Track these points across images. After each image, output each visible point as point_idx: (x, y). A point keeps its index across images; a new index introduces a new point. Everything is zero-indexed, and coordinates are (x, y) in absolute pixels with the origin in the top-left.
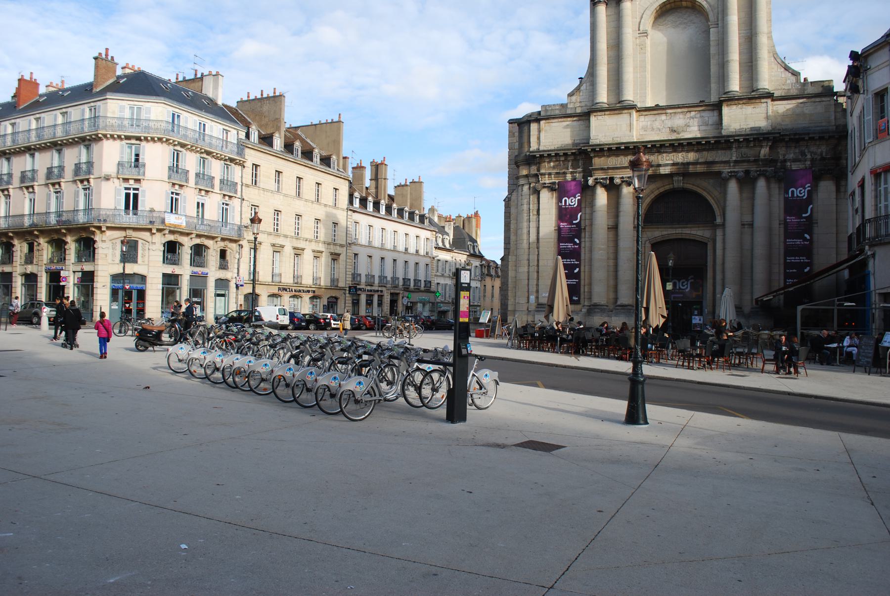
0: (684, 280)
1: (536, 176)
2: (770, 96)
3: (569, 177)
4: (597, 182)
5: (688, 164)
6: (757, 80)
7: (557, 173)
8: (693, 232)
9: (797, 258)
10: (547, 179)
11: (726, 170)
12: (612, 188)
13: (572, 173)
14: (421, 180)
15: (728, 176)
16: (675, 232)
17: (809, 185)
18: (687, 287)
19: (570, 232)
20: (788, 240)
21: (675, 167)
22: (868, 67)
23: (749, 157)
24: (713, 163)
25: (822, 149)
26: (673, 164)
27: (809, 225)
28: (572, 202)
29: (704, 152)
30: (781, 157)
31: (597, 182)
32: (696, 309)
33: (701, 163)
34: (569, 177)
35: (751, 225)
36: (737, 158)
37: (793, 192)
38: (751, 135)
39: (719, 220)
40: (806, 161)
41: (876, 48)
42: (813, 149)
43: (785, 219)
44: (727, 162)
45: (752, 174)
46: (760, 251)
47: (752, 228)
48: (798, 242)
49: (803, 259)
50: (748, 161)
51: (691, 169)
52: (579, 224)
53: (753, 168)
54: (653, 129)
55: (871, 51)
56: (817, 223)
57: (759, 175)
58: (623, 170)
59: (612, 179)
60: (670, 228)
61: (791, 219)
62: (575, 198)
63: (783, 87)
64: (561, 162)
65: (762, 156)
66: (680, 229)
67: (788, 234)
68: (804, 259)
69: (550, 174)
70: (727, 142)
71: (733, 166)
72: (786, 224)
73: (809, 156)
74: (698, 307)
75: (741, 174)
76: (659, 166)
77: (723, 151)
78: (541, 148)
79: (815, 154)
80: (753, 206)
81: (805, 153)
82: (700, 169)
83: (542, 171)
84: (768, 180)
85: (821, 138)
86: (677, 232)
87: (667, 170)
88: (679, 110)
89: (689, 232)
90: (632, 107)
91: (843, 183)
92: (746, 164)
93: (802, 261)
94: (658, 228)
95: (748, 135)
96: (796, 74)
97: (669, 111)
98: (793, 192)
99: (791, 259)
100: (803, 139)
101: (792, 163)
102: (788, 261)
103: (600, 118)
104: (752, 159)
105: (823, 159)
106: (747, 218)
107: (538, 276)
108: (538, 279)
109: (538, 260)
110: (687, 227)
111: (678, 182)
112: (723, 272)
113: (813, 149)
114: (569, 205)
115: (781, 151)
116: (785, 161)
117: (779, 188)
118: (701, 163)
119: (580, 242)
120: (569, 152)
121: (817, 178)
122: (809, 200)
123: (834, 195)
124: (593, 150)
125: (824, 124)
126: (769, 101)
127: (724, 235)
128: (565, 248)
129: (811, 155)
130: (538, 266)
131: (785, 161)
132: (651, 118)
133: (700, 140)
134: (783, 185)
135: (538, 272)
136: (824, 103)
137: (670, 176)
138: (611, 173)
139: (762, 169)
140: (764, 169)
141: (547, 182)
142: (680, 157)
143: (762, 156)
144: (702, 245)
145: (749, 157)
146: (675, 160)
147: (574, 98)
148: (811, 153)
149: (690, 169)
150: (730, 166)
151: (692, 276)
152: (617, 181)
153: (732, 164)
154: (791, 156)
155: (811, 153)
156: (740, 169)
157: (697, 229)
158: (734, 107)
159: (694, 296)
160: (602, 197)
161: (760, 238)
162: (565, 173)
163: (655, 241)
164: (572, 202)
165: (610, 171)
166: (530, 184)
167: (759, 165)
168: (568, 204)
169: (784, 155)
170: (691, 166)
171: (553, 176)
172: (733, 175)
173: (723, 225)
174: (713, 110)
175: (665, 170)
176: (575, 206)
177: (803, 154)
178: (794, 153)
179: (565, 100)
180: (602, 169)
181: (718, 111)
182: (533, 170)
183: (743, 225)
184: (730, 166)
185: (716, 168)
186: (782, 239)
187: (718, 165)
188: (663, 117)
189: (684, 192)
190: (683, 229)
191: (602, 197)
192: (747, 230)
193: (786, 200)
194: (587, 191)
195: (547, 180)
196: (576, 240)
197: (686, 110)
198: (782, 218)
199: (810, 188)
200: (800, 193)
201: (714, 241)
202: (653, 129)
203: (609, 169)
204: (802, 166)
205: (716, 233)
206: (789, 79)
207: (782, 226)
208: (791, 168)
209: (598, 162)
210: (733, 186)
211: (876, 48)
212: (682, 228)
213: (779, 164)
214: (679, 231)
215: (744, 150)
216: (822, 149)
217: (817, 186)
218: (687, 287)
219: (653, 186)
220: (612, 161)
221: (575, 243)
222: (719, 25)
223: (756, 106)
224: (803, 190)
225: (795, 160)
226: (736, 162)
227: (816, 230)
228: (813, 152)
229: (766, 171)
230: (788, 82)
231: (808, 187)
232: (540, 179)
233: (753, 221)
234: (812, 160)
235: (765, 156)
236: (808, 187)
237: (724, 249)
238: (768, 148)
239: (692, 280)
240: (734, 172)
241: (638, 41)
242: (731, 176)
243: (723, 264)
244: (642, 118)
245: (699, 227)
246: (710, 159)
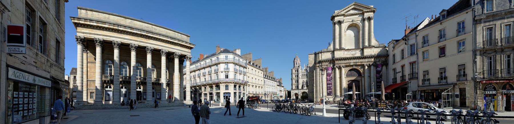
1: (321, 66)
2: (374, 47)
3: (329, 66)
4: (336, 67)
5: (357, 62)
6: (371, 43)
7: (326, 65)
12: (340, 68)
13: (330, 65)
24: (362, 62)
25: (383, 59)
26: (354, 62)
27: (381, 76)
31: (336, 67)
33: (360, 62)
34: (329, 66)
39: (363, 75)
42: (382, 59)
43: (376, 75)
48: (379, 80)
51: (358, 64)
54: (348, 54)
59: (340, 66)
67: (377, 79)
69: (324, 65)
72: (377, 76)
73: (381, 61)
76: (351, 63)
78: (322, 59)
82: (359, 64)
83: (322, 65)
85: (384, 57)
90: (344, 49)
97: (352, 50)
99: (378, 84)
111: (354, 67)
112: (364, 87)
113: (382, 59)
118: (360, 62)
120: (329, 60)
121: (382, 66)
122: (381, 71)
123: (386, 70)
124: (336, 59)
126: (374, 48)
127: (364, 79)
137: (352, 66)
138: (340, 65)
142: (355, 61)
152: (341, 67)
154: (377, 61)
158: (367, 49)
160: (337, 71)
162: (328, 65)
166: (319, 68)
173: (364, 77)
175: (352, 64)
177: (380, 60)
180: (338, 64)
182: (320, 64)
185: (363, 63)
186: (376, 79)
188: (350, 52)
191: (337, 71)
193: (376, 70)
194: (333, 69)
198: (376, 75)
200: (379, 69)
201: (362, 80)
202: (348, 54)
203: (339, 64)
204: (379, 63)
209: (336, 62)
217: (382, 68)
219: (348, 68)
220: (340, 62)
221: (331, 81)
225: (378, 62)
226: (367, 62)
227: (382, 77)
234: (382, 62)
241: (344, 33)
243: (364, 85)
244: (346, 52)
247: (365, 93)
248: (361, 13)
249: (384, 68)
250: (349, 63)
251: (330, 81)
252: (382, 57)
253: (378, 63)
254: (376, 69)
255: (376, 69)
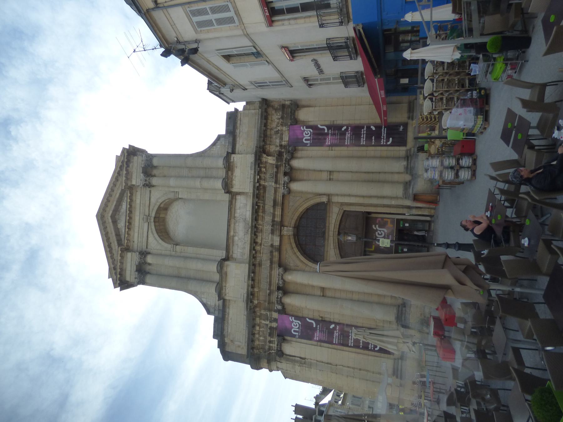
0: (377, 233)
5: (273, 221)
8: (334, 221)
9: (362, 137)
10: (274, 345)
11: (281, 191)
14: (294, 405)
15: (287, 189)
16: (332, 237)
17: (302, 127)
18: (383, 231)
19: (323, 331)
20: (346, 144)
21: (275, 232)
22: (176, 39)
23: (274, 172)
25: (275, 118)
28: (295, 326)
29: (266, 208)
30: (278, 149)
32: (404, 225)
35: (331, 172)
36: (273, 182)
37: (306, 140)
38: (255, 169)
39: (324, 199)
40: (282, 130)
41: (158, 32)
43: (329, 146)
44: (276, 190)
45: (288, 170)
46: (354, 165)
47: (333, 172)
49: (364, 131)
50: (277, 173)
51: (278, 219)
52: (317, 321)
53: (282, 169)
55: (160, 35)
56: (333, 121)
57: (289, 165)
58: (273, 276)
60: (328, 241)
61: (328, 142)
62: (293, 322)
63: (227, 147)
64: (261, 329)
65: (274, 162)
66: (330, 232)
67: (341, 144)
68: (364, 131)
70: (258, 188)
71: (279, 185)
72: (332, 145)
73: (279, 128)
74: (401, 222)
75: (286, 179)
77: (267, 193)
79: (278, 123)
80: (314, 170)
81: (277, 131)
82: (278, 212)
84: (293, 157)
85: (266, 118)
86: (332, 235)
87: (277, 239)
88: (232, 225)
89: (333, 225)
91: (304, 103)
92: (279, 175)
93: (365, 132)
94: (327, 251)
95: (255, 172)
96: (219, 137)
97: (232, 233)
98: (306, 140)
100: (265, 131)
101: (284, 140)
102: (364, 143)
103: (227, 291)
104: (275, 170)
105: (282, 118)
106: (325, 176)
107: (364, 370)
108: (368, 371)
109: (348, 367)
110: (329, 227)
111: (288, 231)
112: (371, 197)
113: (274, 125)
114: (299, 328)
115: (273, 148)
116: (281, 146)
117: (302, 150)
119: (334, 323)
122: (314, 128)
123: (312, 109)
125: (257, 118)
127: (337, 195)
128: (338, 339)
129: (279, 126)
130: (354, 368)
131: (281, 146)
132: (235, 248)
133: (255, 210)
134: (300, 148)
135: (360, 370)
136: (242, 118)
139: (284, 162)
140: (284, 160)
141: (276, 345)
143: (274, 162)
144: (346, 215)
145: (274, 172)
146: (269, 232)
147: (212, 310)
148: (277, 126)
149: (278, 220)
150: (279, 188)
151: (374, 226)
153: (278, 186)
154: (278, 141)
155: (277, 126)
156: (283, 179)
157: (331, 218)
158: (234, 182)
159: (392, 226)
161: (342, 165)
163: (339, 255)
164: (297, 325)
165: (272, 288)
167: (281, 164)
168: (298, 330)
169: (277, 146)
170: (276, 219)
171: (272, 339)
172: (286, 185)
173: (329, 195)
174: (236, 199)
176: (300, 323)
177: (277, 132)
178: (276, 138)
179: (212, 318)
181: (237, 196)
183: (330, 179)
184: (279, 188)
185: (280, 199)
186: (345, 148)
187: (277, 197)
188: (236, 238)
189: (297, 228)
190: (330, 230)
192: (335, 176)
193: (312, 145)
195: (274, 345)
196: (332, 326)
197: (233, 221)
198: (327, 148)
199: (305, 127)
200: (307, 134)
201: (342, 204)
203: (270, 289)
205: (335, 202)
206: (222, 143)
207: (334, 148)
208: (287, 141)
210: (295, 186)
211: (158, 32)
212: (329, 231)
213: (283, 150)
214: (331, 233)
215: (268, 176)
216: (275, 118)
218: (383, 231)
221: (334, 328)
222: (177, 191)
223: (236, 165)
224: (306, 132)
225: (281, 139)
226: (276, 182)
227: (339, 122)
228: (277, 125)
229: (286, 159)
230: (223, 143)
231: (303, 128)
232: (273, 351)
233: (328, 171)
235: (274, 160)
236: (303, 128)
237: (349, 195)
238: (269, 158)
239: (377, 226)
240: (284, 184)
242: (287, 187)
243: (363, 197)
245: (329, 217)
246: (272, 203)
247: (397, 198)
248: (129, 195)
249: (302, 115)
250: (271, 252)
251: (331, 333)
252: (266, 125)
253: (286, 138)
254: (306, 145)
255: (306, 145)
